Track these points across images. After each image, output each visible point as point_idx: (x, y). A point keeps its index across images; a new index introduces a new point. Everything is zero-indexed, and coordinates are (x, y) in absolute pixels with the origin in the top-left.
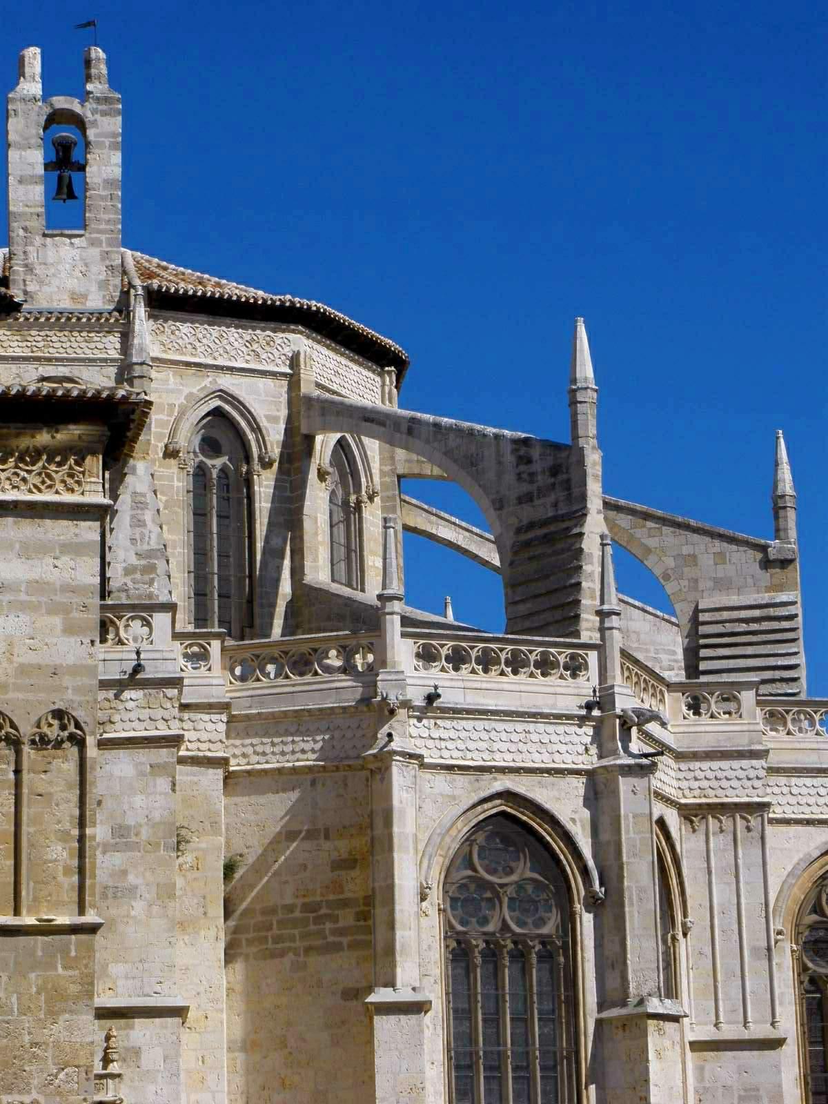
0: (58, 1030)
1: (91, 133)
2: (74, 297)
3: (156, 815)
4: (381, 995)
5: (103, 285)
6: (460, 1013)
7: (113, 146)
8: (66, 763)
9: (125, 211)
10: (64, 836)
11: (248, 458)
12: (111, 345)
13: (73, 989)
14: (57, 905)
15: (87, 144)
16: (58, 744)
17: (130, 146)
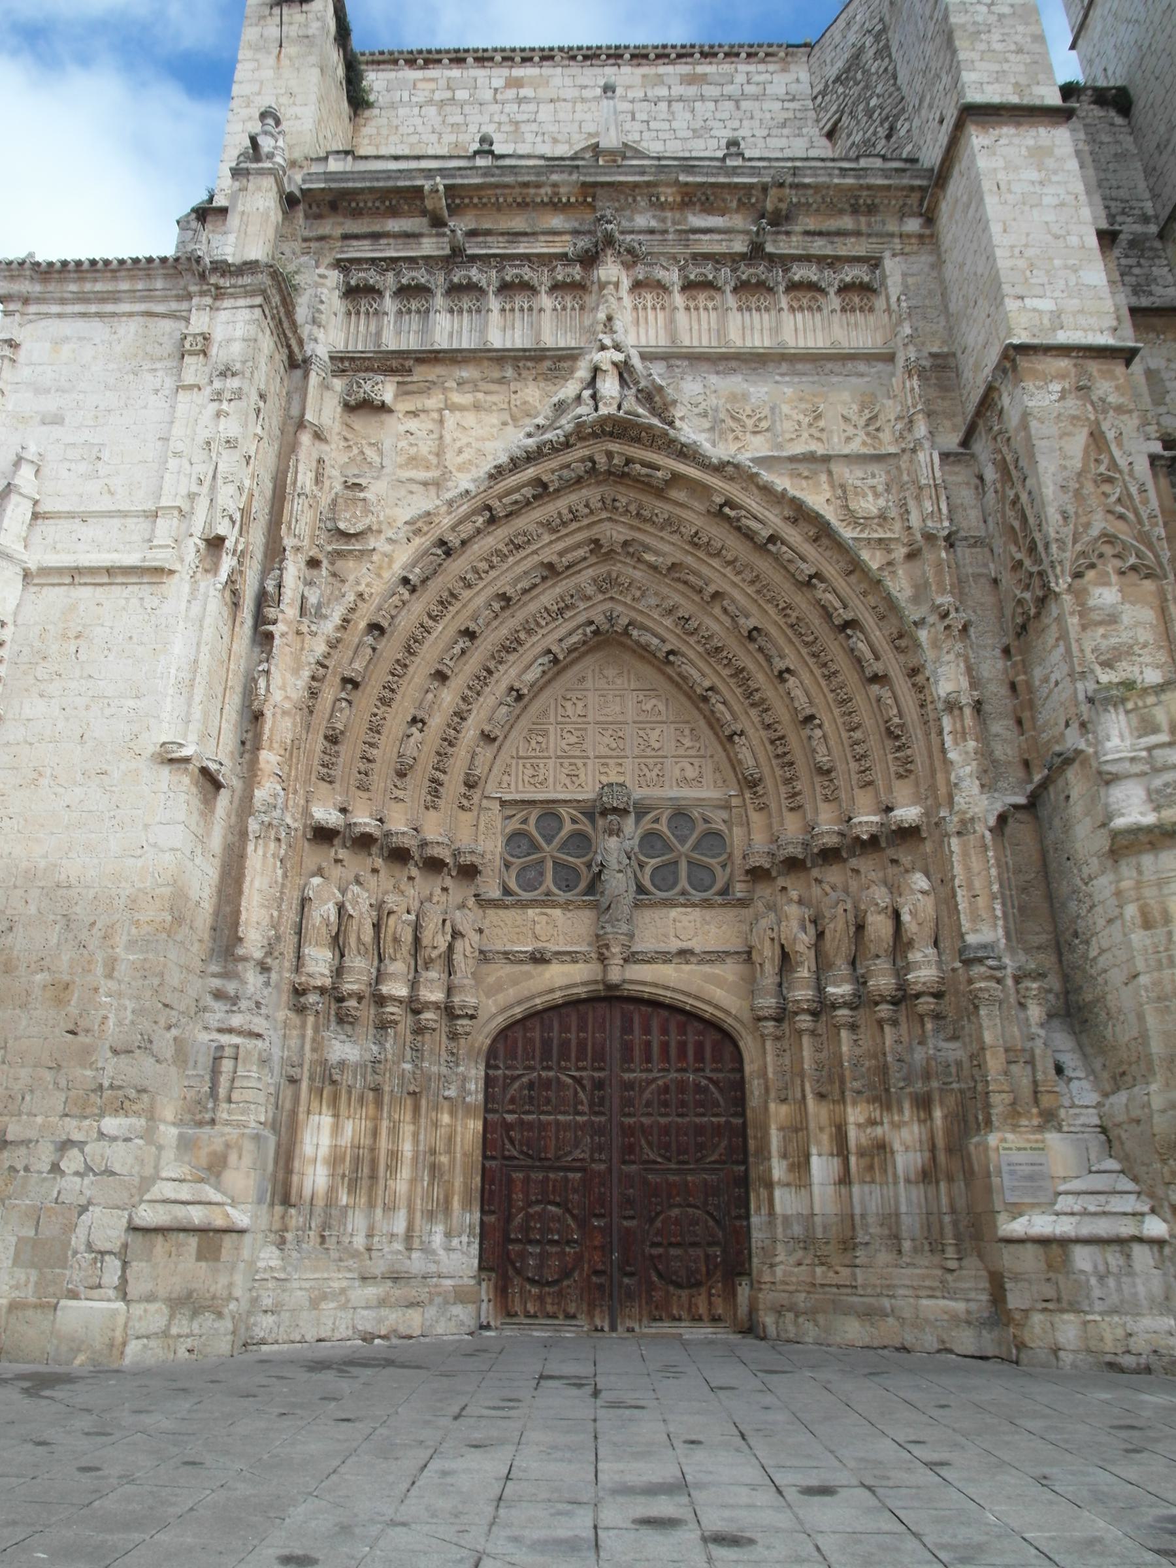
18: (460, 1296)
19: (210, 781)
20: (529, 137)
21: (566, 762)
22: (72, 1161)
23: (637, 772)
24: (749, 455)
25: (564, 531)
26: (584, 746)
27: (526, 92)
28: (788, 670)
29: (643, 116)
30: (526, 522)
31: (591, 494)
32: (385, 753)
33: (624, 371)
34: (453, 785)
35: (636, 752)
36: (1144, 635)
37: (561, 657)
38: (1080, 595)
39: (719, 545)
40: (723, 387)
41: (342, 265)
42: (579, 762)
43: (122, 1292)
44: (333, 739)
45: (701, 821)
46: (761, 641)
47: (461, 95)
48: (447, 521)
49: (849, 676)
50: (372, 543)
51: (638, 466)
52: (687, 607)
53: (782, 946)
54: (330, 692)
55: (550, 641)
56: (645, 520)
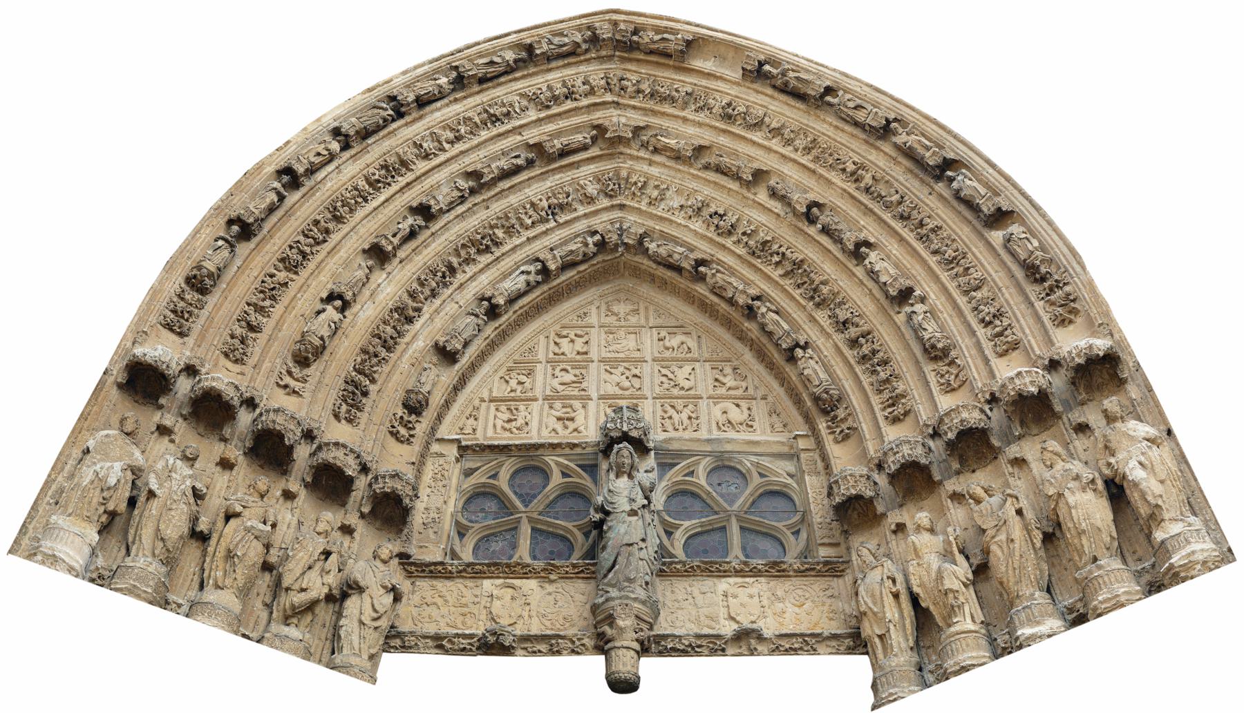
21: (558, 404)
23: (659, 413)
25: (555, 110)
26: (584, 385)
28: (868, 244)
30: (506, 93)
31: (594, 72)
35: (657, 390)
37: (552, 266)
39: (761, 113)
42: (577, 404)
45: (755, 475)
46: (824, 219)
49: (958, 228)
51: (651, 34)
52: (722, 196)
53: (915, 600)
55: (536, 248)
56: (664, 99)
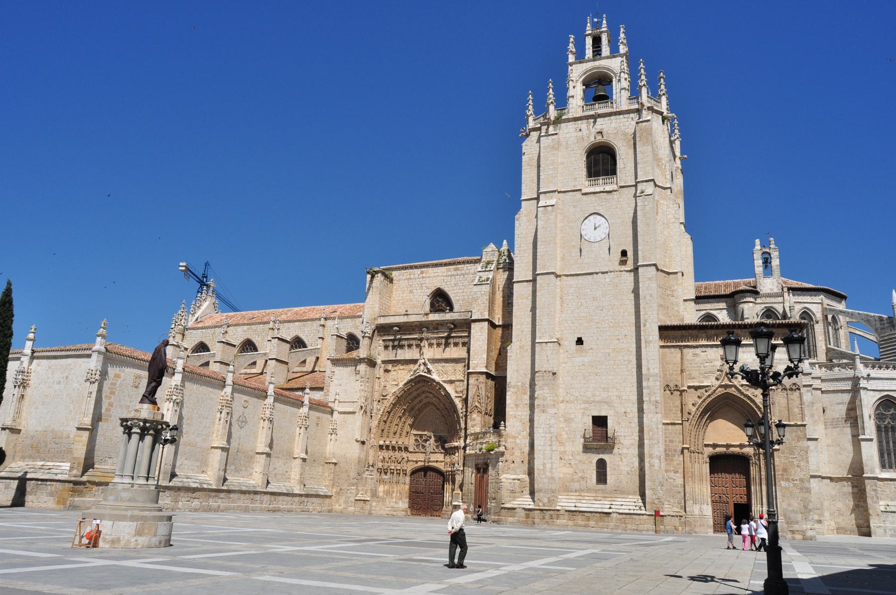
0: (800, 444)
1: (772, 256)
2: (771, 290)
3: (809, 400)
4: (861, 437)
5: (777, 287)
6: (880, 442)
7: (777, 258)
8: (797, 393)
9: (780, 269)
10: (798, 407)
11: (813, 321)
12: (780, 299)
13: (802, 436)
14: (797, 420)
15: (771, 258)
16: (795, 390)
17: (781, 257)
18: (403, 511)
19: (363, 443)
20: (424, 288)
22: (349, 492)
24: (444, 379)
27: (424, 275)
29: (445, 281)
32: (392, 431)
33: (425, 364)
34: (404, 433)
36: (479, 422)
38: (471, 416)
40: (439, 366)
41: (384, 341)
43: (354, 506)
44: (383, 431)
47: (412, 276)
48: (398, 393)
50: (388, 397)
54: (381, 423)
